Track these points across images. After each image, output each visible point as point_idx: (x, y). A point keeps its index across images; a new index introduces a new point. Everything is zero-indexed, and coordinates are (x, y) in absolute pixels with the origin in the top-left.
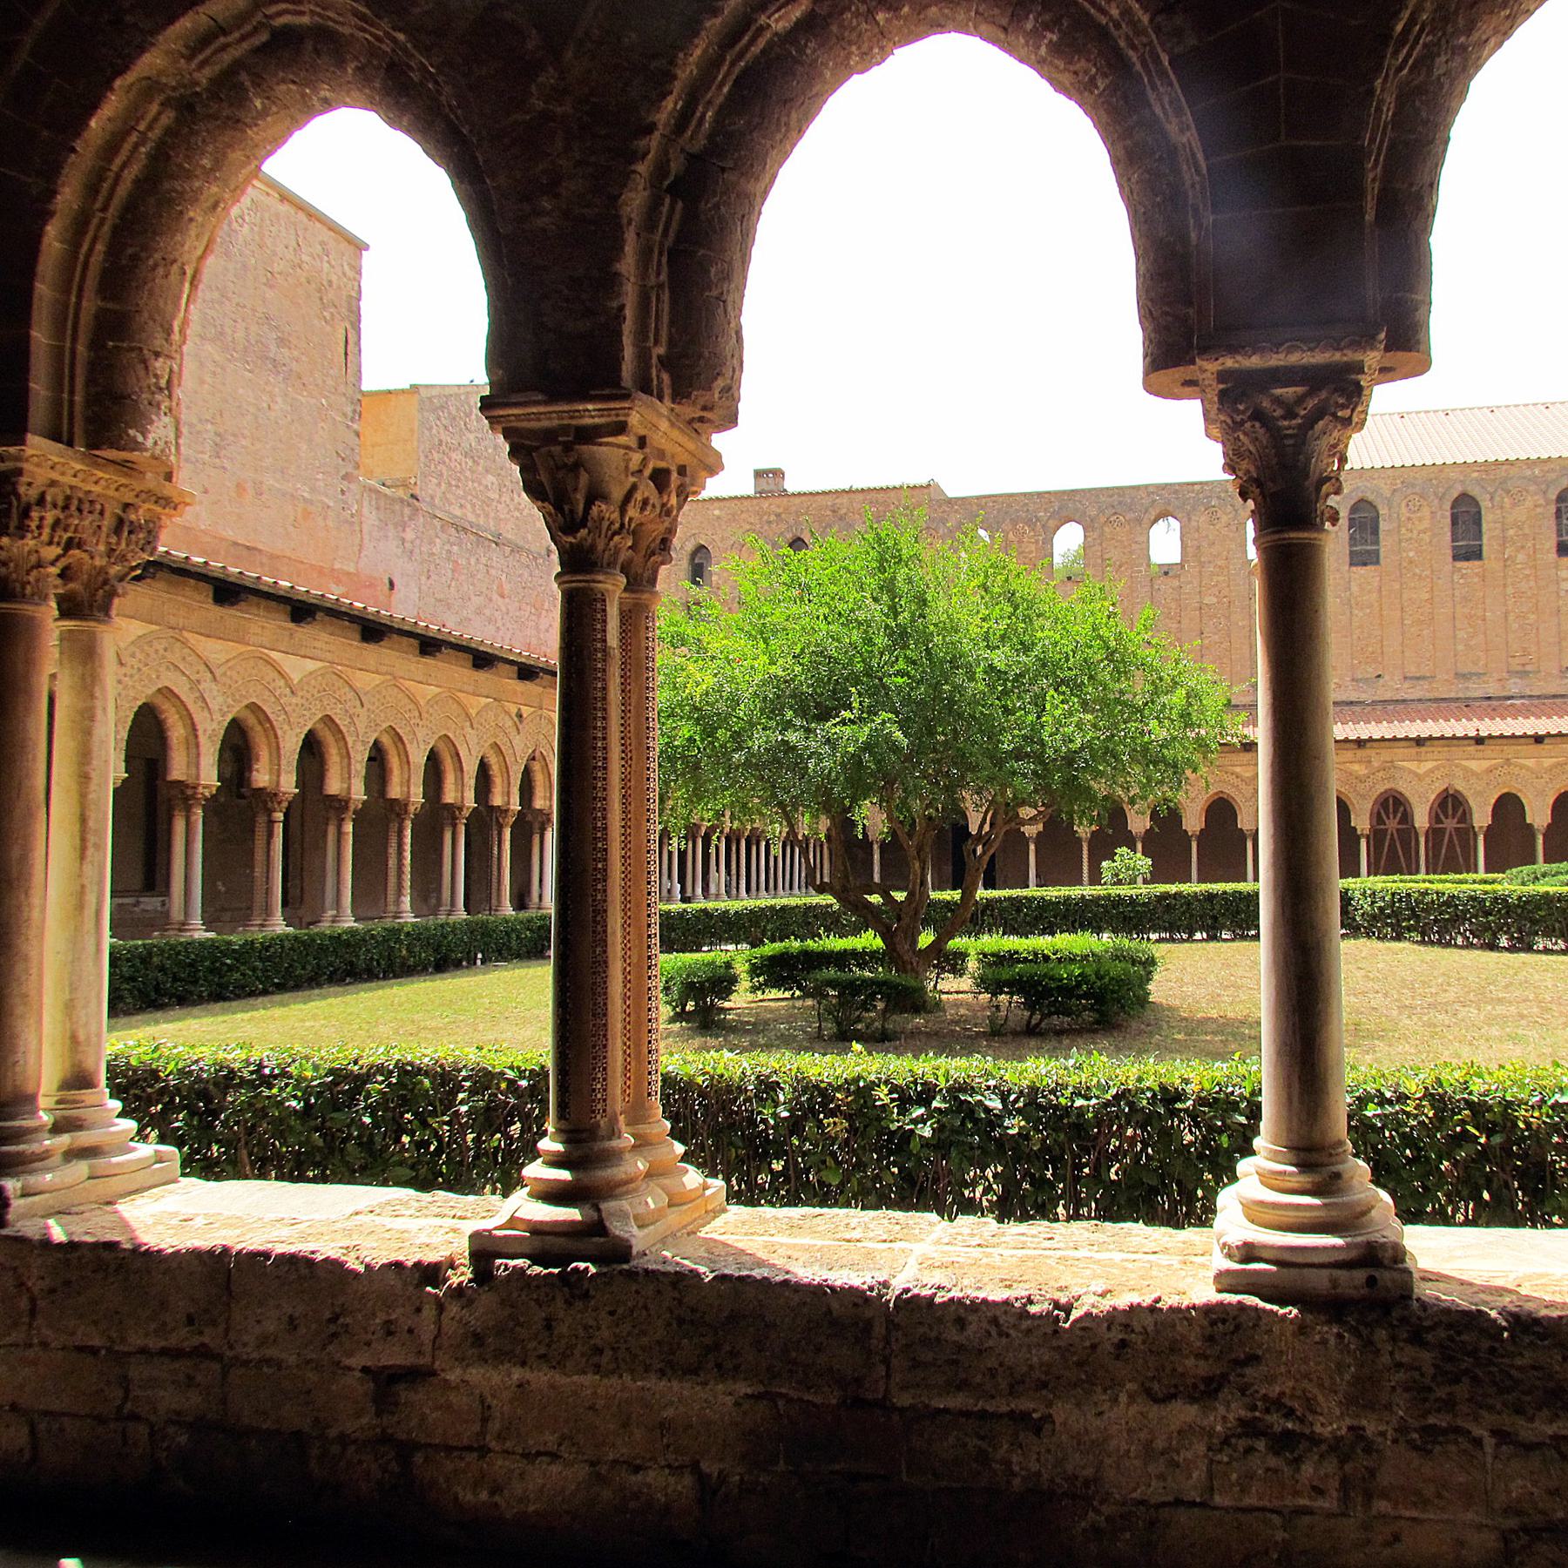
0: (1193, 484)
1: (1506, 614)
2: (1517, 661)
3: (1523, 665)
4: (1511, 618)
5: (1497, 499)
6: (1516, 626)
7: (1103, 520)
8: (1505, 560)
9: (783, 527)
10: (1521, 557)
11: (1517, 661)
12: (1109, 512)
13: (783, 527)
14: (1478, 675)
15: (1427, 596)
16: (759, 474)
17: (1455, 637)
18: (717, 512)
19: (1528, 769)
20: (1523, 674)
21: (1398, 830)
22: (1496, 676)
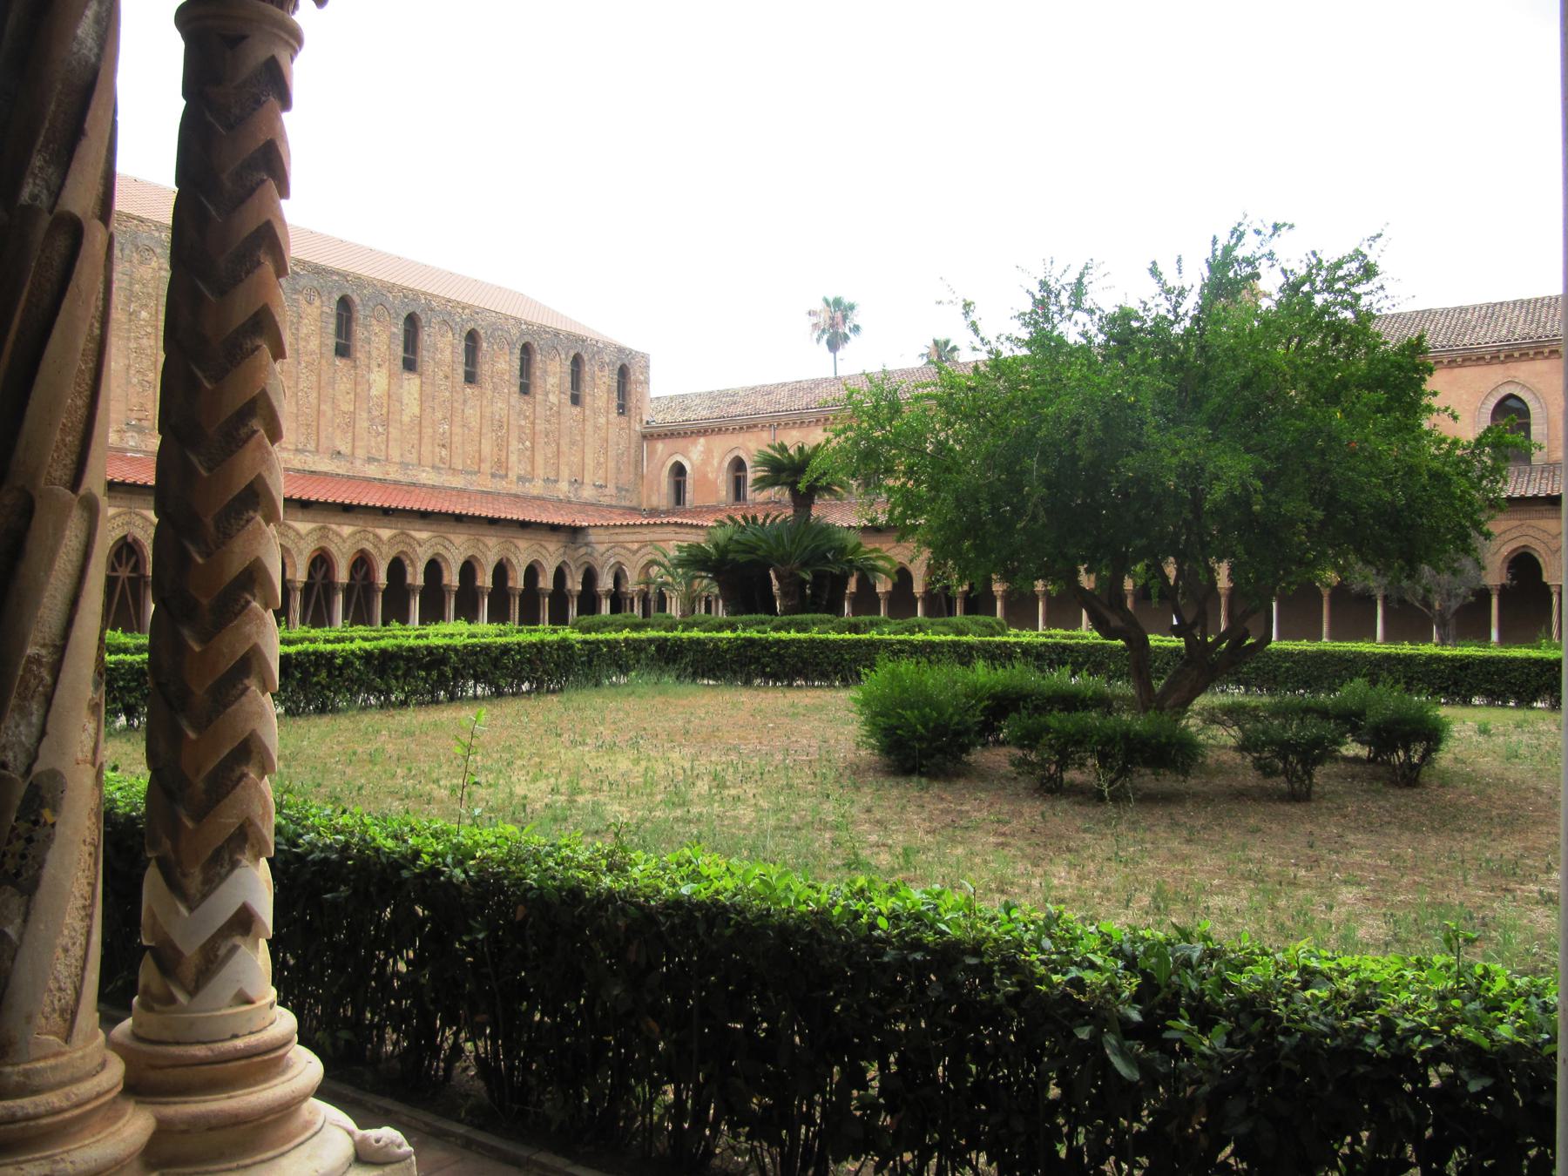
1: (129, 367)
2: (134, 415)
3: (140, 420)
4: (132, 372)
6: (135, 381)
8: (131, 314)
10: (144, 314)
11: (134, 415)
21: (118, 578)
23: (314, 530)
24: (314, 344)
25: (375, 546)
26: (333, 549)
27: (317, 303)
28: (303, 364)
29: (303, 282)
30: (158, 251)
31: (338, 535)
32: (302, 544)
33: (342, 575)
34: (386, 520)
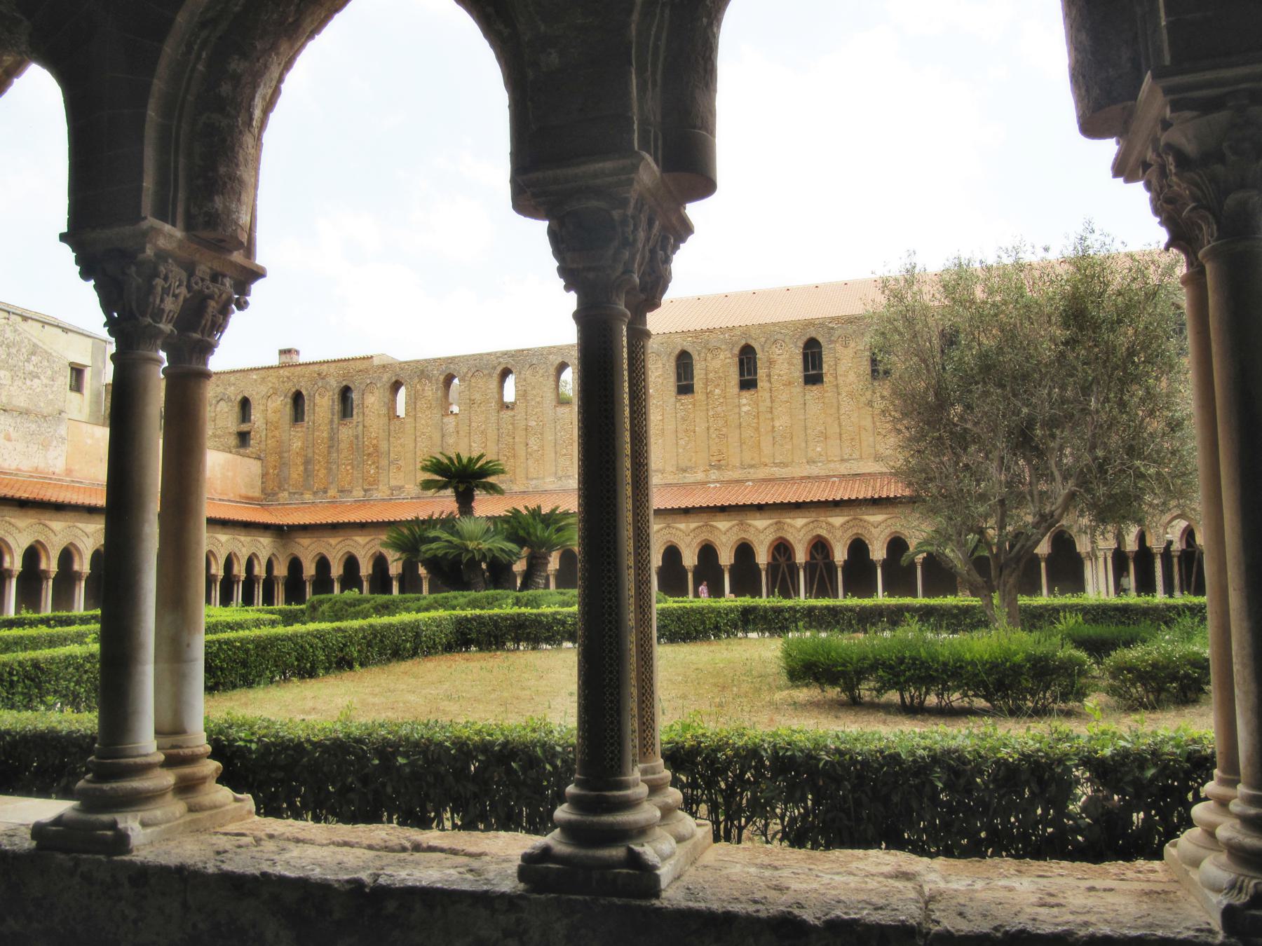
0: (523, 351)
1: (708, 429)
2: (715, 458)
4: (712, 430)
5: (703, 355)
6: (714, 436)
7: (470, 375)
9: (291, 384)
10: (717, 391)
11: (715, 458)
12: (473, 370)
13: (291, 384)
14: (691, 468)
15: (661, 418)
16: (284, 352)
17: (677, 444)
18: (255, 377)
19: (680, 530)
20: (719, 468)
22: (702, 469)
23: (772, 525)
24: (852, 377)
25: (829, 532)
26: (790, 538)
27: (852, 344)
28: (844, 394)
29: (837, 333)
30: (723, 347)
31: (792, 526)
32: (762, 537)
33: (801, 557)
34: (838, 510)
